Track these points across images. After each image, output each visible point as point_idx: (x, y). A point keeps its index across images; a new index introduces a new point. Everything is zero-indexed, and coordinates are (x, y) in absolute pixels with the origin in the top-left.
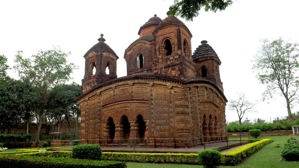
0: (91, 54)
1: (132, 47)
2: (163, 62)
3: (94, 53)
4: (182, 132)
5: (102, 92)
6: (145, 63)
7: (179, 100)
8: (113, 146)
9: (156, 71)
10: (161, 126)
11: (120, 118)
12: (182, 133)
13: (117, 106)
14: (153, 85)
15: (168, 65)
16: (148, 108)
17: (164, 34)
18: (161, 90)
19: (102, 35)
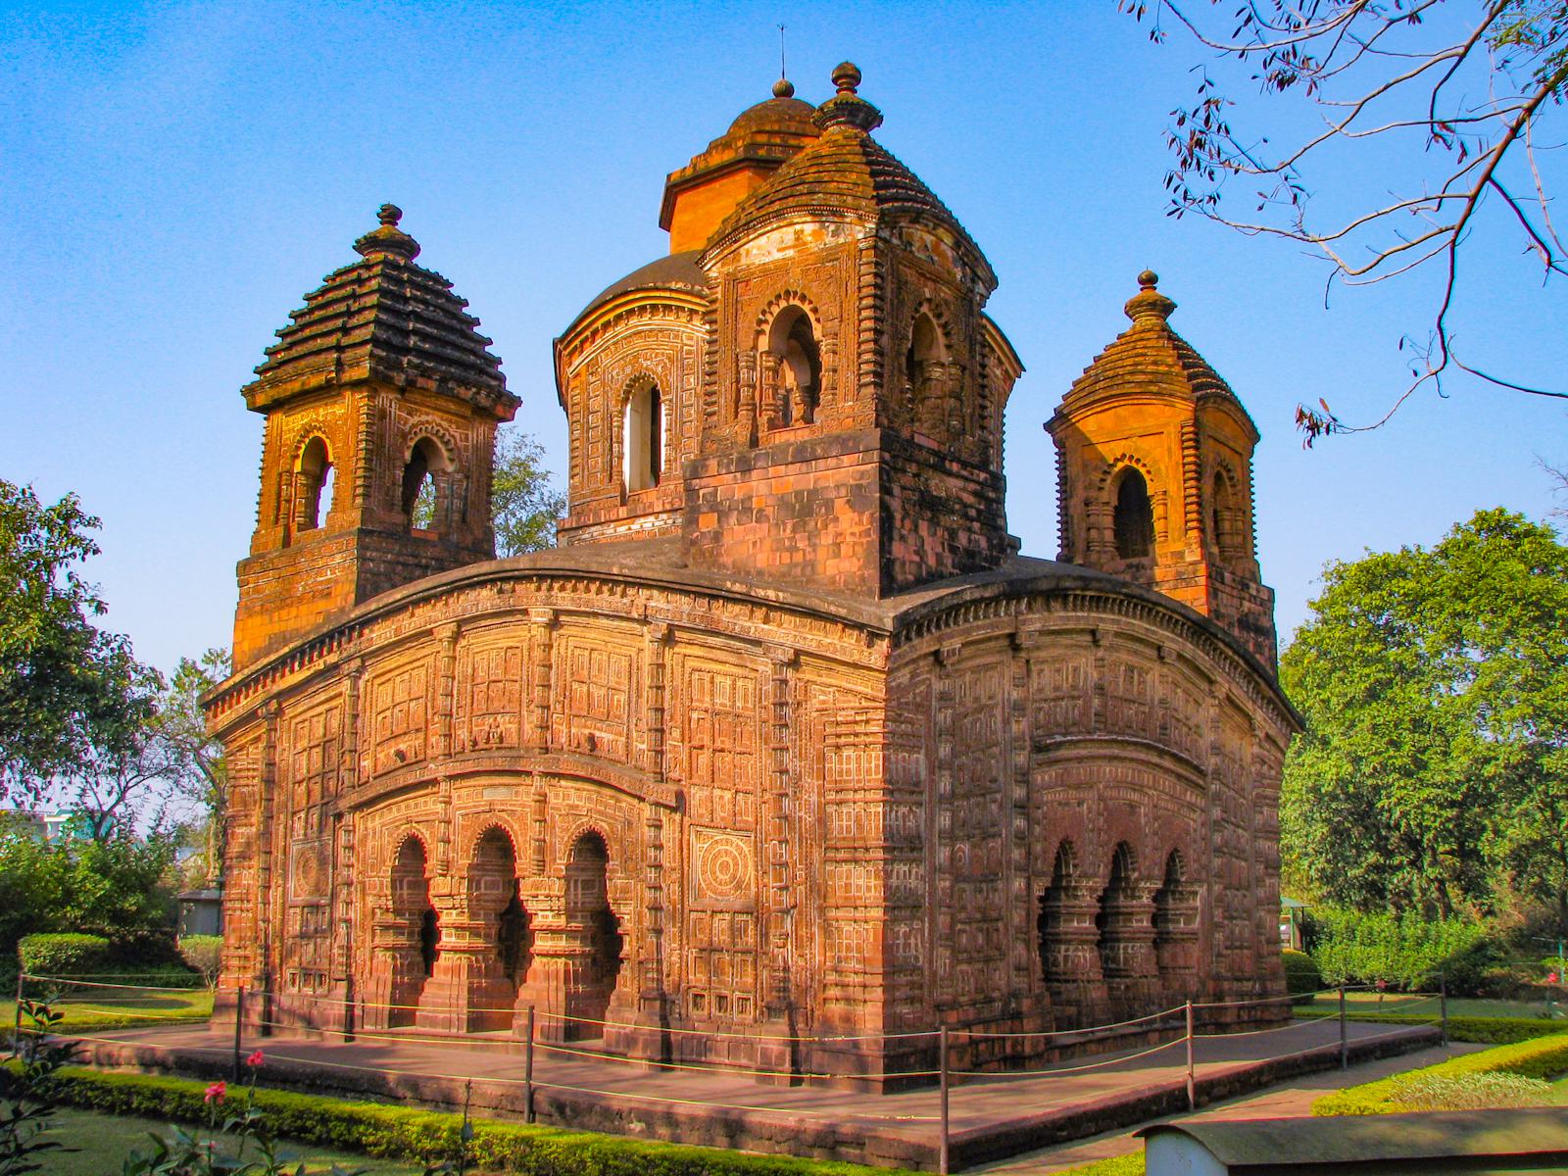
3: (949, 253)
8: (1093, 1047)
13: (1107, 769)
18: (1233, 741)
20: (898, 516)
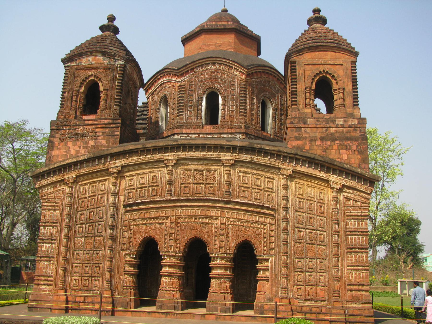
0: (90, 58)
1: (193, 69)
2: (318, 126)
4: (359, 291)
5: (128, 166)
6: (224, 117)
7: (354, 219)
9: (300, 143)
10: (307, 274)
11: (182, 244)
12: (359, 293)
13: (180, 212)
14: (292, 176)
15: (332, 134)
16: (273, 227)
17: (319, 63)
19: (112, 19)
20: (57, 143)
